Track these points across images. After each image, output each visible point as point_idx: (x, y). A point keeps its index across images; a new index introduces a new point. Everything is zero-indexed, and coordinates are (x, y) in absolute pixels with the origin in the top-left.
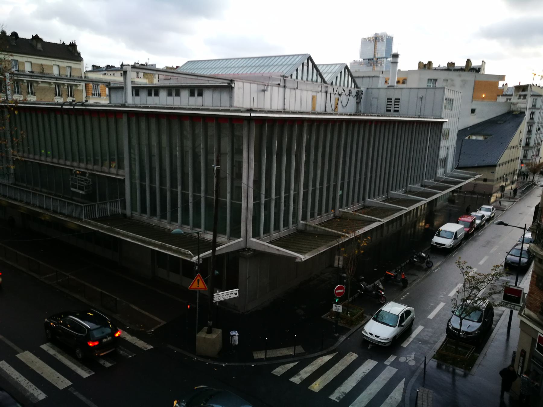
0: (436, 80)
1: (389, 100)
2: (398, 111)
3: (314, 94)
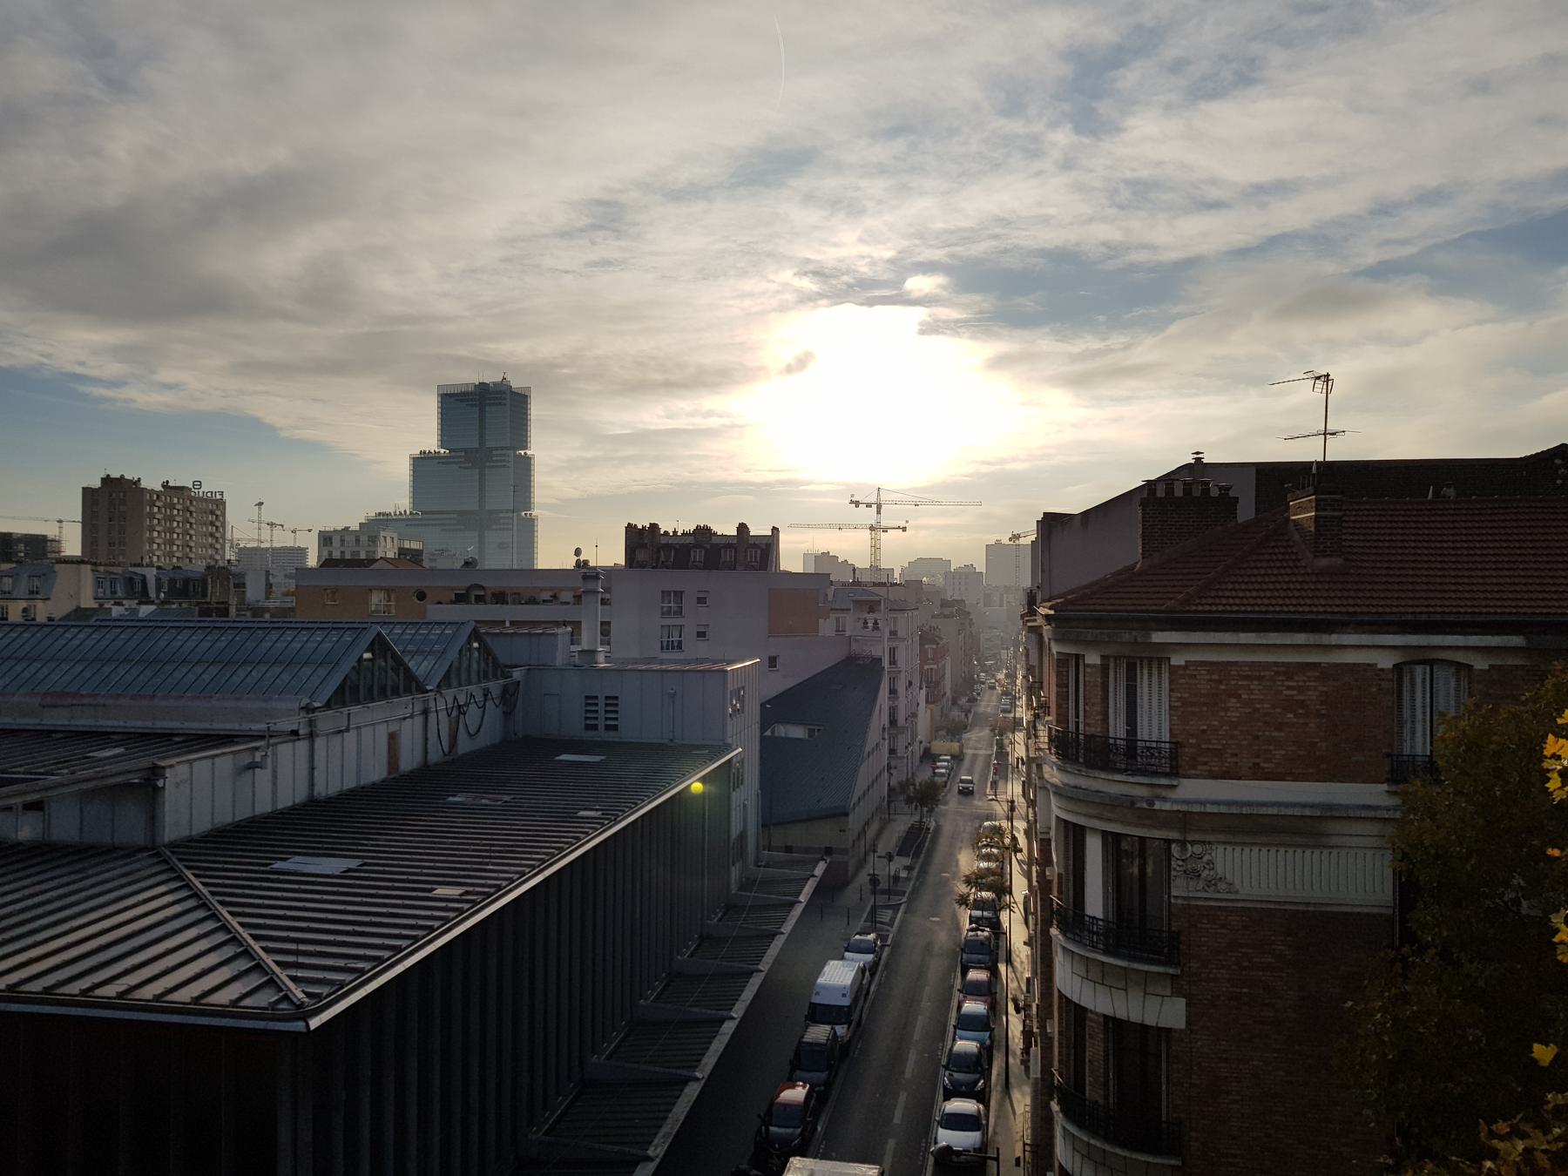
0: (679, 595)
1: (591, 699)
2: (615, 728)
3: (393, 728)
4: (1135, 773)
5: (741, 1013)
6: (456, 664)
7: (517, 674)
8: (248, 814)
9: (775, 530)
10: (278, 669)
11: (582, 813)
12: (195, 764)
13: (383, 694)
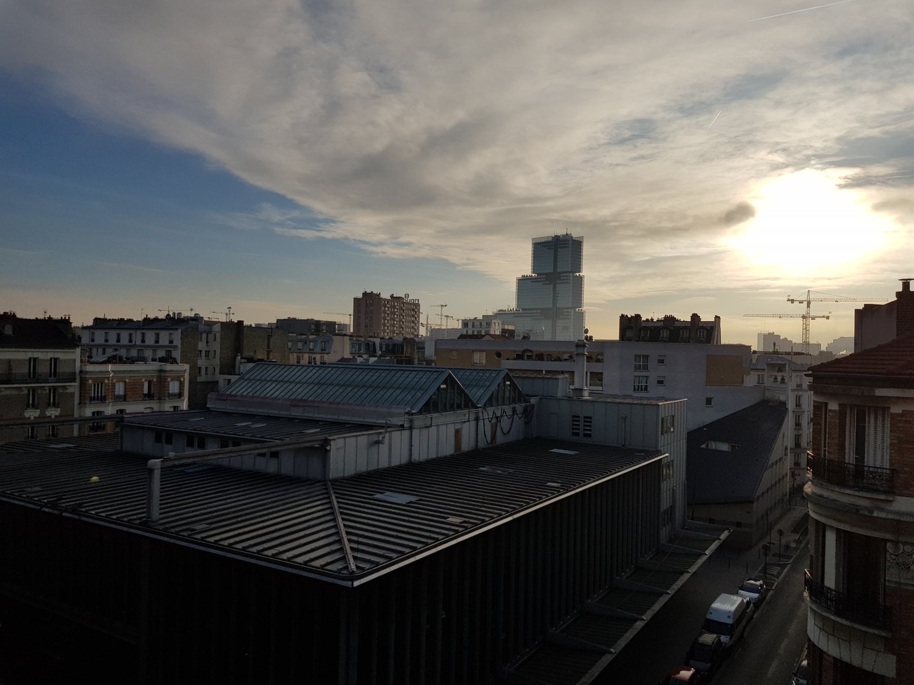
0: (646, 357)
1: (575, 418)
3: (458, 426)
4: (861, 489)
6: (495, 393)
7: (533, 401)
8: (376, 468)
9: (717, 318)
10: (398, 392)
11: (549, 484)
12: (347, 439)
13: (452, 408)
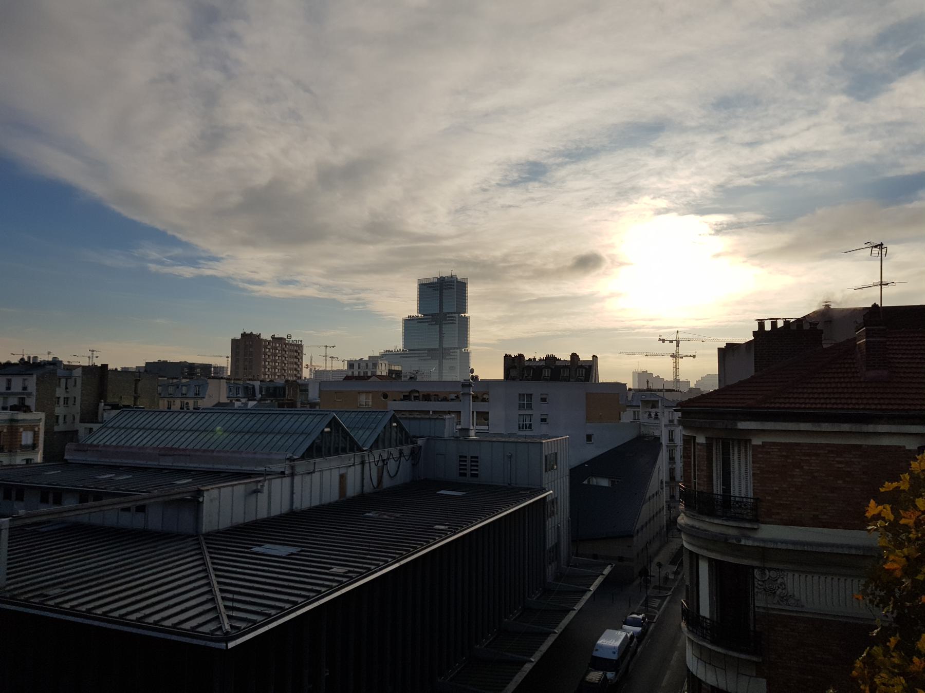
0: (530, 396)
1: (462, 458)
2: (476, 476)
3: (343, 471)
4: (729, 519)
5: (537, 660)
7: (420, 442)
9: (595, 357)
10: (279, 437)
11: (437, 527)
12: (222, 490)
13: (337, 452)
